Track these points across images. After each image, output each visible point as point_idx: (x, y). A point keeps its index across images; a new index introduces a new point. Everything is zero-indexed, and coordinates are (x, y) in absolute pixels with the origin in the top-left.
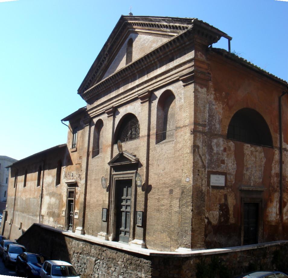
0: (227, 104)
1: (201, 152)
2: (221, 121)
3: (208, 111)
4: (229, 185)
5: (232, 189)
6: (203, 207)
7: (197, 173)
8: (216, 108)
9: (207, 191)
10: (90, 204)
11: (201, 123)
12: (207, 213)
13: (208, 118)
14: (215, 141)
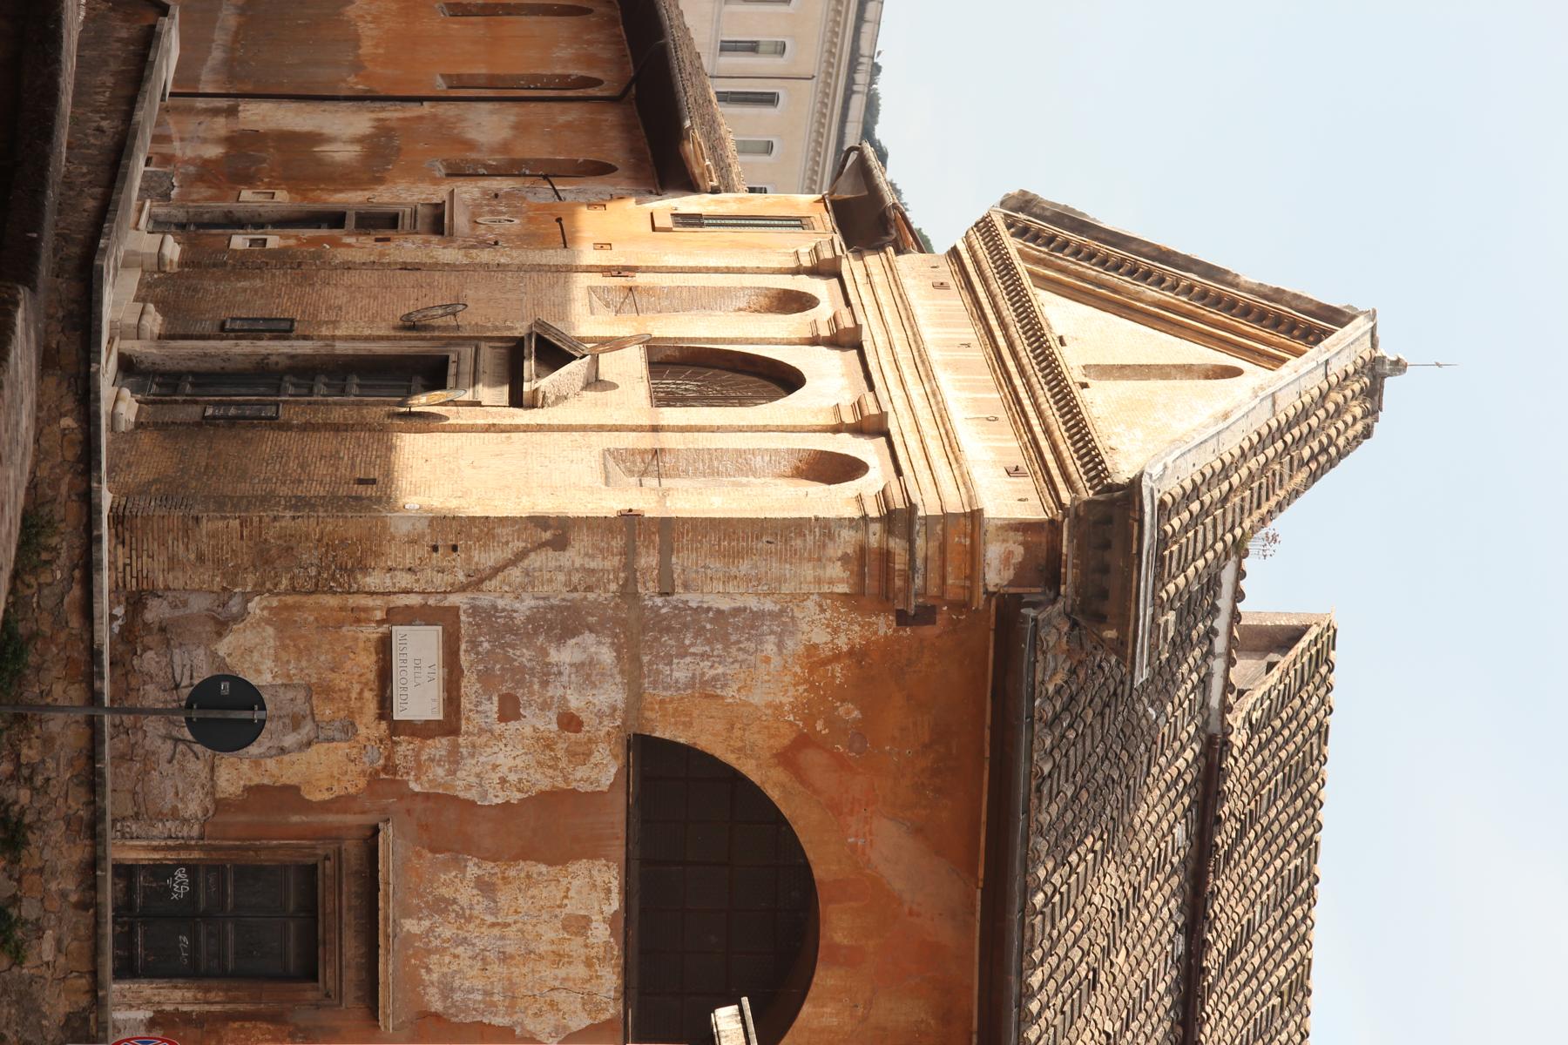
0: (804, 741)
1: (537, 565)
2: (707, 696)
3: (745, 609)
4: (401, 749)
5: (383, 776)
6: (292, 578)
7: (440, 543)
8: (767, 660)
9: (366, 610)
10: (318, 287)
11: (674, 559)
12: (262, 609)
13: (709, 609)
14: (607, 655)
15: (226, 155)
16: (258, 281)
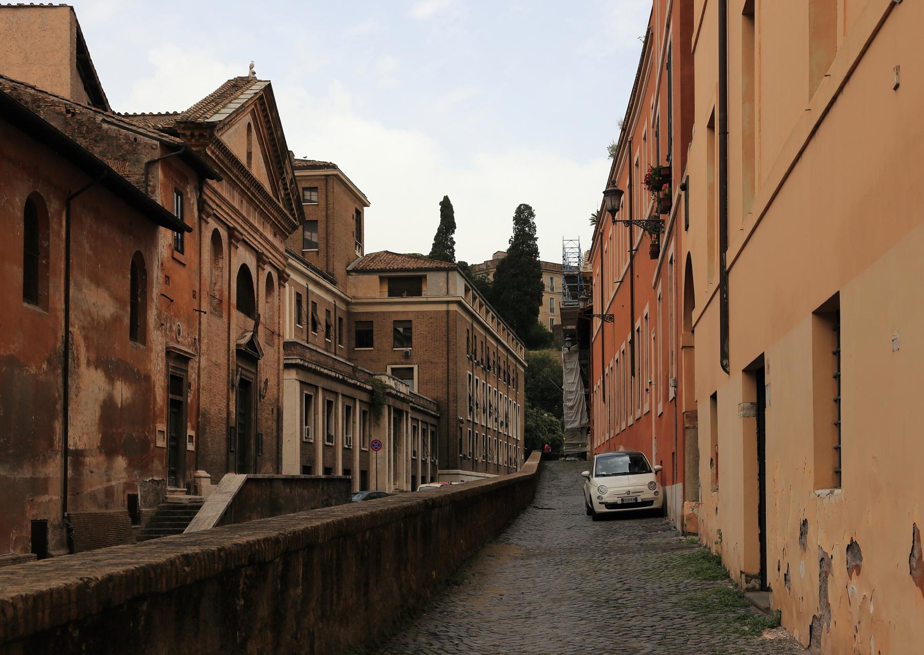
15: (123, 455)
16: (208, 439)
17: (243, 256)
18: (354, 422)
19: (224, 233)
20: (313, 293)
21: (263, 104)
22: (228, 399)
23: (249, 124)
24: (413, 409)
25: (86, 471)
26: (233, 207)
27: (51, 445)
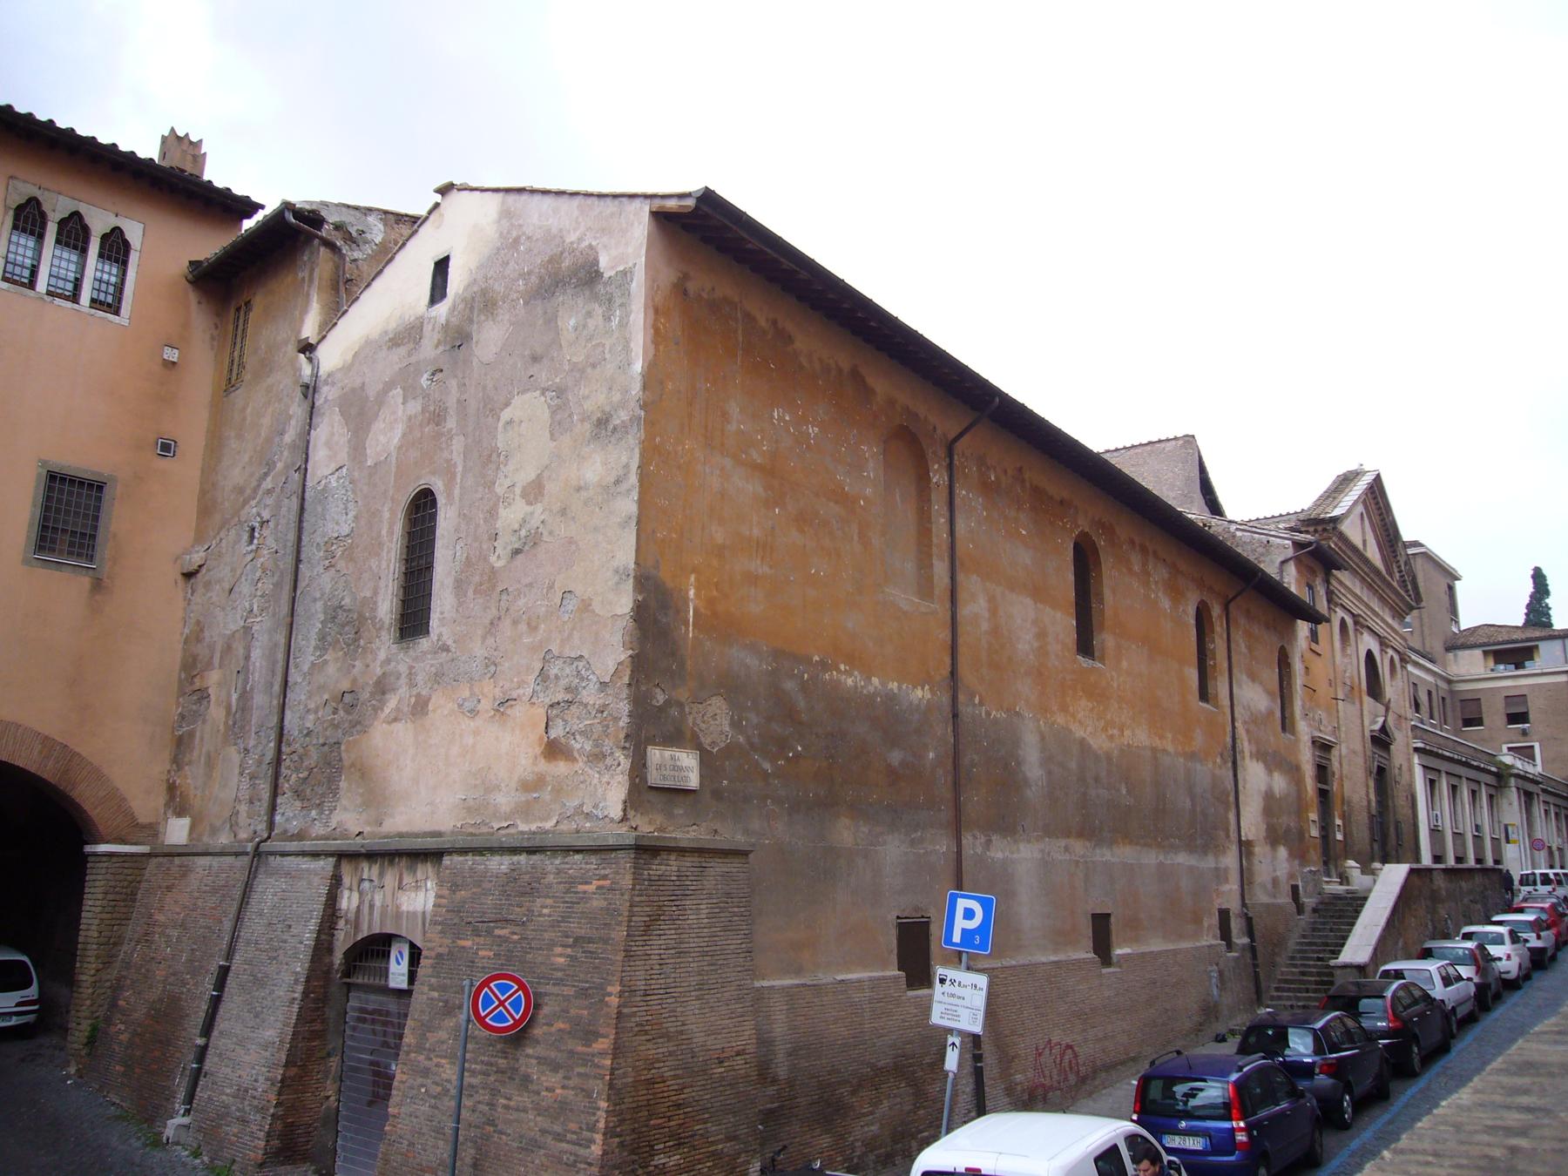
15: (1284, 845)
17: (1369, 642)
18: (1481, 807)
19: (1349, 621)
20: (1412, 674)
21: (1373, 493)
22: (1367, 786)
23: (1362, 514)
24: (1544, 791)
25: (1256, 862)
26: (1356, 595)
27: (1228, 836)
